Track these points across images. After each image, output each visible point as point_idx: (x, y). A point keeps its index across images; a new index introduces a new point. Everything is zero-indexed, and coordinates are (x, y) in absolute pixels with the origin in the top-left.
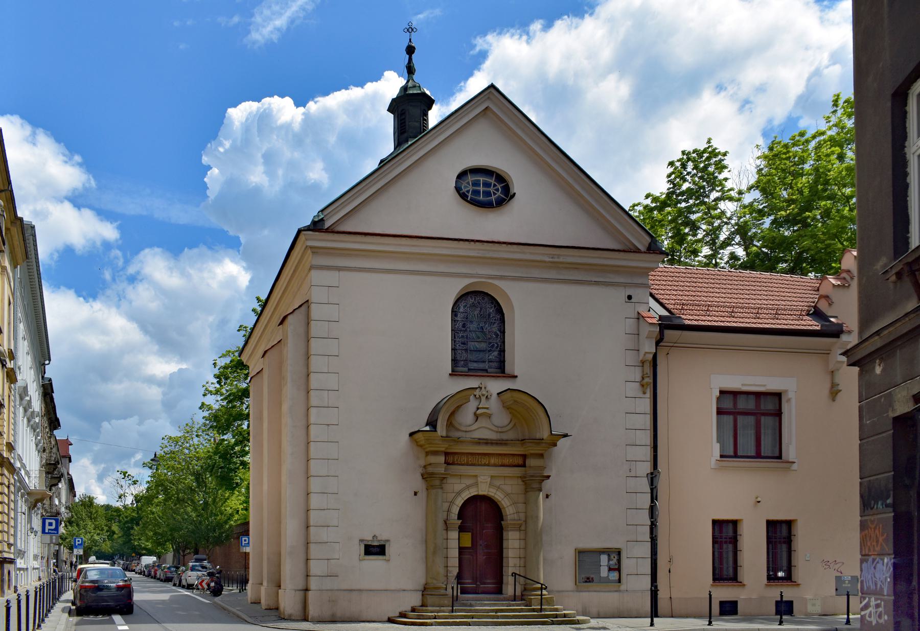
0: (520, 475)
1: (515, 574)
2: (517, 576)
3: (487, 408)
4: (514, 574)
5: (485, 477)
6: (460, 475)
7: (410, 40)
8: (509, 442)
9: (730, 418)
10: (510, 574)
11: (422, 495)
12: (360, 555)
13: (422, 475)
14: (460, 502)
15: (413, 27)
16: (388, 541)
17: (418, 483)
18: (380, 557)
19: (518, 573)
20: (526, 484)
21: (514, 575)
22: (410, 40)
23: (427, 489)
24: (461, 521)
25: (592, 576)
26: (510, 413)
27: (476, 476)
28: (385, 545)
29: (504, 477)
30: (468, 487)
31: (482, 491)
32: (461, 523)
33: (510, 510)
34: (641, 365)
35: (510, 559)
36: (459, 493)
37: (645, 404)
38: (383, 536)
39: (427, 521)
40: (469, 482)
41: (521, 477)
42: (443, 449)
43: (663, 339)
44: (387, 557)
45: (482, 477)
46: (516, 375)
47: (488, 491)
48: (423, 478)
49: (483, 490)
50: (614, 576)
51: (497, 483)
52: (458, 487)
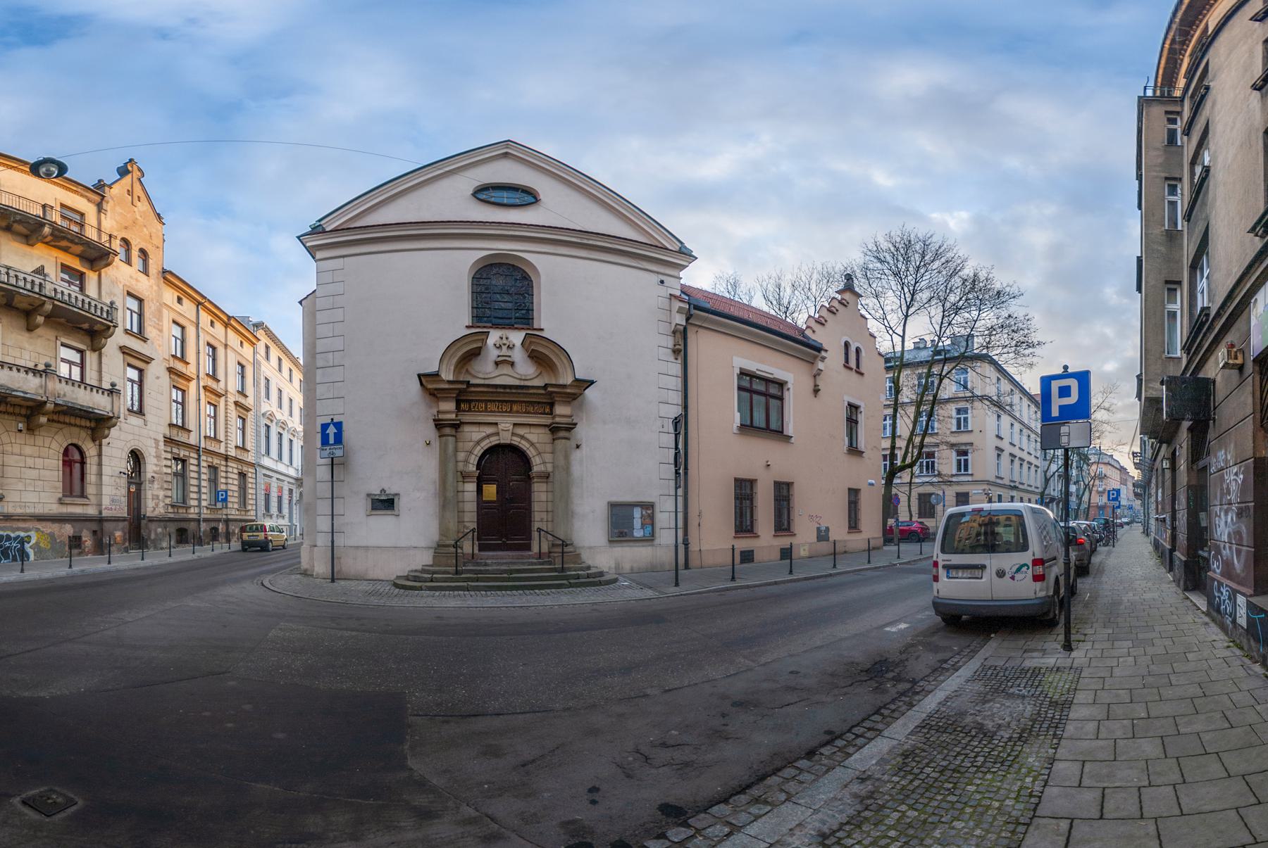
2: (542, 533)
3: (510, 356)
4: (539, 530)
5: (507, 425)
11: (436, 444)
14: (478, 451)
17: (430, 432)
18: (389, 512)
27: (496, 424)
36: (478, 443)
38: (392, 490)
40: (490, 430)
44: (396, 513)
45: (503, 425)
49: (506, 438)
51: (521, 431)
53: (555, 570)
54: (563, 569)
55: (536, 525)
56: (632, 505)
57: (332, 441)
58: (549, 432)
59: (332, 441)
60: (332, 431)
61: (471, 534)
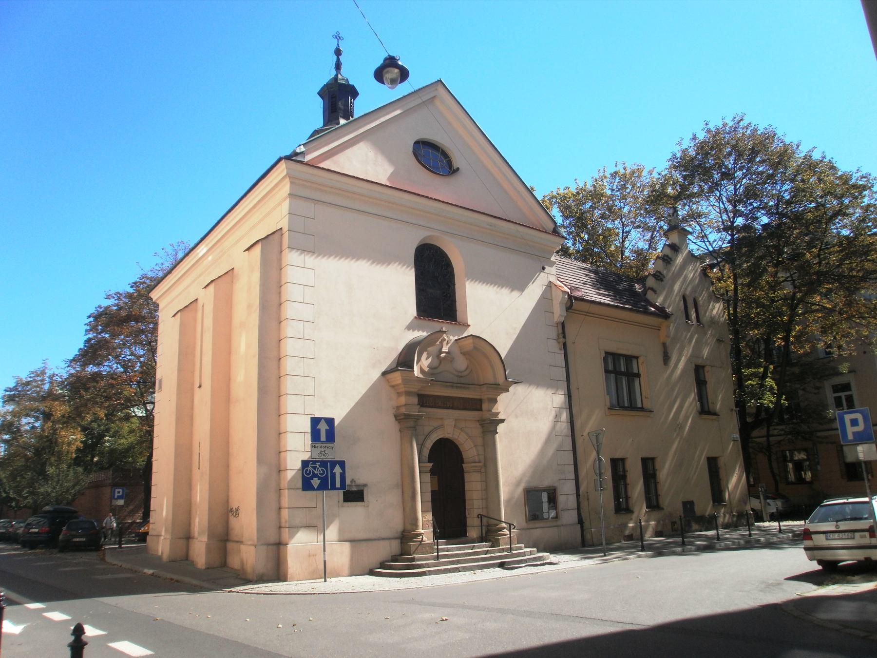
0: (478, 419)
1: (482, 516)
6: (429, 418)
7: (338, 44)
9: (613, 375)
10: (476, 515)
12: (339, 502)
13: (396, 416)
15: (340, 36)
16: (365, 485)
19: (485, 513)
20: (482, 427)
21: (480, 516)
22: (338, 44)
23: (400, 431)
24: (432, 464)
26: (467, 359)
27: (442, 419)
28: (363, 490)
30: (436, 429)
33: (469, 450)
35: (474, 501)
39: (402, 465)
41: (478, 421)
42: (416, 390)
43: (572, 307)
46: (469, 324)
47: (453, 434)
48: (396, 420)
50: (553, 514)
52: (427, 429)
53: (503, 550)
54: (511, 549)
56: (330, 490)
57: (323, 437)
58: (478, 426)
59: (323, 437)
60: (323, 427)
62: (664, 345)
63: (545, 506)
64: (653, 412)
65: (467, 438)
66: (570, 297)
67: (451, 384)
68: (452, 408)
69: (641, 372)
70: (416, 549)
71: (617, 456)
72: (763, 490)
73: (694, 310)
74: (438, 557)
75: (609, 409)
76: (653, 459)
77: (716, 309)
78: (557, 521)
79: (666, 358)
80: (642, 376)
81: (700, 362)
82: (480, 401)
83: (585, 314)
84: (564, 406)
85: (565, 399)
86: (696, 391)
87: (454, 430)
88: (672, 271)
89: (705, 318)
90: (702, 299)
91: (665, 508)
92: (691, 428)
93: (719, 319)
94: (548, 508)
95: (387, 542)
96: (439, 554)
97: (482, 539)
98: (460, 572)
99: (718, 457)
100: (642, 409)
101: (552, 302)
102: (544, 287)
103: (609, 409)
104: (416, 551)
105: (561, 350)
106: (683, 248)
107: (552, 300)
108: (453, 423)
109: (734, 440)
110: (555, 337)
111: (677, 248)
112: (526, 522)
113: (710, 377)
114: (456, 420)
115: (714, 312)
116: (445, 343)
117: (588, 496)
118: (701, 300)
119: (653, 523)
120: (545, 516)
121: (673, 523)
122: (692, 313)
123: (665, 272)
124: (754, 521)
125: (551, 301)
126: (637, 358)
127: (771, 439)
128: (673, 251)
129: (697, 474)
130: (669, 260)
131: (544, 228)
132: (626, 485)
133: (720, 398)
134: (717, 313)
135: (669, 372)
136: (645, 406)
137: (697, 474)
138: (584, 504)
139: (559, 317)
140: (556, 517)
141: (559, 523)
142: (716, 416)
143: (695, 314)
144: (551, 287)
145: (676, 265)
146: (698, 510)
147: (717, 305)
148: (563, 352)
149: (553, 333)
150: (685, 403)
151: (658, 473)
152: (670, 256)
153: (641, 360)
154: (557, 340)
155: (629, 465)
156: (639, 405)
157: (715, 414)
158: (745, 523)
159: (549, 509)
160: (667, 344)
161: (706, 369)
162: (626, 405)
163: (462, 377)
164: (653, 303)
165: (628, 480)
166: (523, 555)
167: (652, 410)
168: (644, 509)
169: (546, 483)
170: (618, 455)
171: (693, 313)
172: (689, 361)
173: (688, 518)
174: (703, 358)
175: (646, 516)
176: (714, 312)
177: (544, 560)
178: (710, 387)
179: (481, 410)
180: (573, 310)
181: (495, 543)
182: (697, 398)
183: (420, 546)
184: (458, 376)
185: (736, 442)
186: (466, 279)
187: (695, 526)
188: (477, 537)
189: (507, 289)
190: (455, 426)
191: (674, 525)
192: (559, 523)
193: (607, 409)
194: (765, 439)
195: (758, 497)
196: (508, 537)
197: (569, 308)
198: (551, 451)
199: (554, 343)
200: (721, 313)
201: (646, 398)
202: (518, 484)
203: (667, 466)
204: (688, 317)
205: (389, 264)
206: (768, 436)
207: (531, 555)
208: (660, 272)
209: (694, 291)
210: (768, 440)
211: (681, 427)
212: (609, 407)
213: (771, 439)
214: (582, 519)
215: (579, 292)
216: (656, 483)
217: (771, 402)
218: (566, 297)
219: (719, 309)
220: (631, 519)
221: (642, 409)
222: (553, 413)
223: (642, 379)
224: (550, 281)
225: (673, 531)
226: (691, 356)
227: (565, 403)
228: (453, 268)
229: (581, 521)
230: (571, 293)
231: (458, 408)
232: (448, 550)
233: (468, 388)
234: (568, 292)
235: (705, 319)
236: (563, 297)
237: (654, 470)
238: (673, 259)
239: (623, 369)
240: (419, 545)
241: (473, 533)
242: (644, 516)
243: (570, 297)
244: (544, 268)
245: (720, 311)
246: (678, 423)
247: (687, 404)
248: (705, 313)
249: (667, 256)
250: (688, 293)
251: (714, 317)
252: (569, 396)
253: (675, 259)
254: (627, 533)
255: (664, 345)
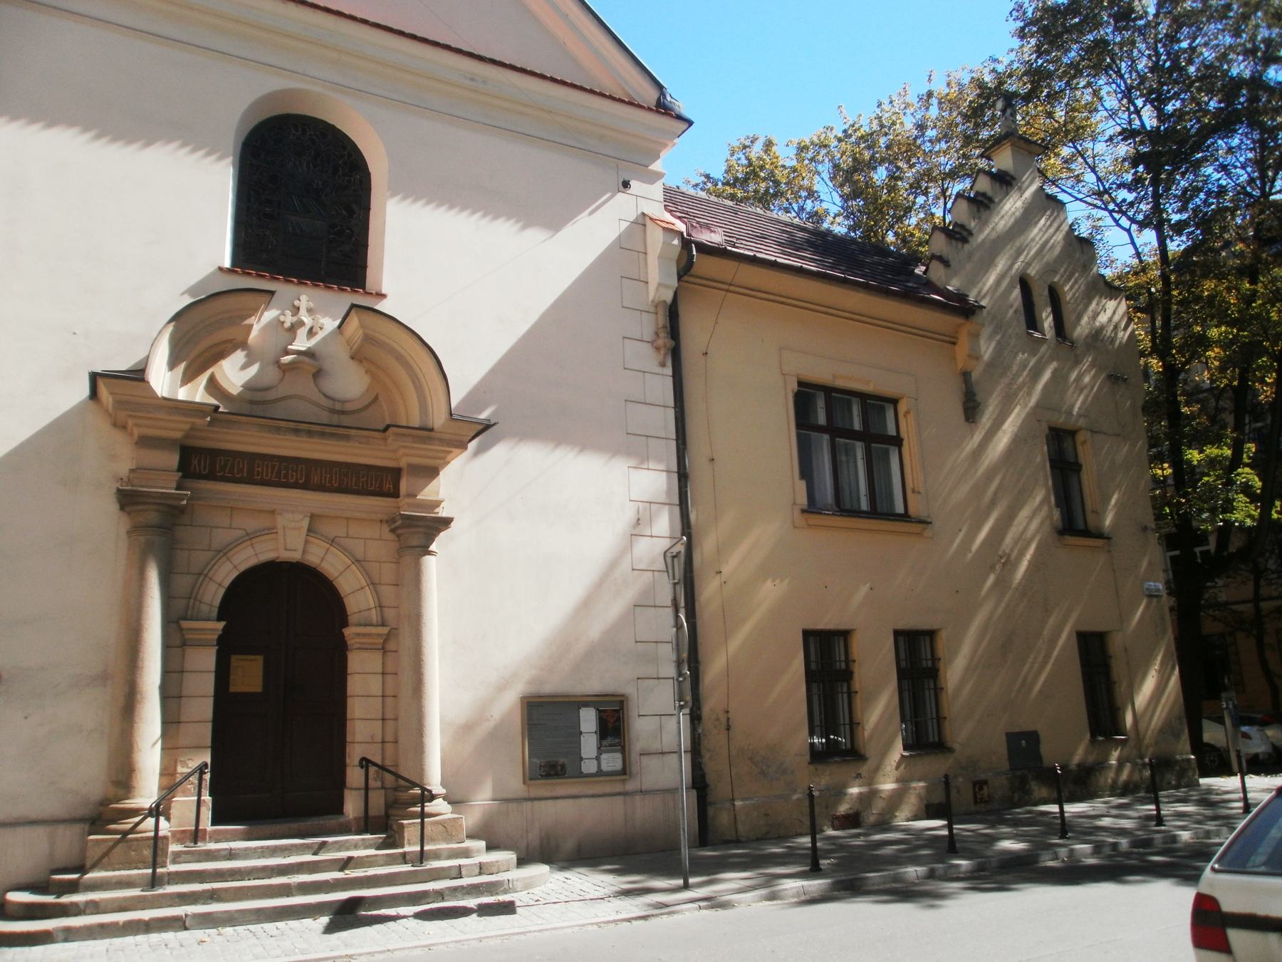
0: (381, 516)
2: (372, 770)
4: (365, 763)
8: (353, 432)
10: (356, 761)
19: (378, 760)
20: (398, 536)
21: (364, 762)
25: (561, 760)
26: (366, 372)
29: (348, 519)
31: (286, 549)
32: (223, 630)
34: (652, 310)
37: (663, 386)
46: (384, 292)
47: (304, 551)
50: (612, 761)
53: (404, 858)
54: (422, 856)
55: (354, 753)
58: (389, 535)
61: (194, 779)
62: (966, 375)
63: (589, 745)
64: (931, 523)
65: (349, 562)
66: (686, 243)
67: (292, 425)
68: (305, 486)
69: (903, 434)
70: (106, 854)
71: (821, 626)
72: (1231, 706)
73: (1049, 310)
74: (154, 881)
75: (803, 511)
76: (931, 634)
77: (1109, 313)
78: (624, 781)
79: (971, 409)
80: (905, 443)
81: (1060, 420)
82: (396, 473)
83: (732, 288)
84: (663, 498)
85: (669, 478)
86: (1050, 483)
87: (307, 542)
88: (994, 224)
89: (1079, 330)
90: (1072, 288)
91: (957, 747)
92: (1035, 566)
93: (1116, 334)
94: (599, 748)
95: (40, 833)
96: (159, 870)
97: (367, 824)
98: (186, 929)
99: (1110, 632)
100: (905, 517)
101: (646, 259)
102: (624, 225)
103: (803, 511)
104: (105, 860)
105: (663, 365)
106: (1024, 179)
107: (646, 253)
108: (305, 524)
109: (1150, 596)
110: (648, 333)
111: (1008, 178)
112: (524, 783)
113: (1095, 455)
114: (313, 516)
115: (1103, 318)
116: (302, 333)
117: (728, 719)
118: (1069, 291)
119: (922, 784)
120: (589, 767)
121: (979, 785)
122: (1044, 315)
123: (973, 225)
124: (1197, 777)
125: (642, 256)
126: (894, 402)
127: (1263, 605)
128: (998, 185)
129: (1049, 667)
130: (986, 201)
131: (629, 95)
132: (851, 694)
133: (1113, 501)
134: (1110, 320)
135: (978, 437)
136: (912, 511)
137: (1049, 667)
138: (715, 740)
139: (657, 289)
140: (624, 771)
141: (631, 786)
142: (1100, 540)
143: (1051, 318)
144: (645, 225)
145: (1003, 212)
146: (1050, 753)
147: (1111, 305)
148: (669, 371)
149: (647, 325)
150: (1021, 507)
151: (941, 665)
152: (990, 193)
153: (902, 407)
154: (652, 343)
155: (858, 646)
156: (900, 509)
157: (1099, 535)
158: (1173, 782)
159: (600, 750)
160: (975, 376)
161: (1080, 437)
162: (864, 505)
163: (343, 412)
164: (942, 287)
165: (856, 685)
166: (454, 873)
167: (929, 520)
168: (897, 751)
169: (594, 684)
170: (827, 622)
171: (1047, 317)
172: (1034, 415)
173: (1019, 773)
174: (1070, 413)
175: (903, 766)
176: (1103, 318)
177: (506, 892)
178: (1089, 478)
179: (396, 494)
180: (692, 276)
181: (393, 840)
182: (1053, 499)
183: (120, 846)
184: (332, 411)
185: (1155, 600)
186: (388, 194)
187: (1040, 791)
188: (355, 819)
189: (512, 221)
190: (309, 530)
191: (981, 789)
192: (631, 786)
193: (797, 512)
194: (1250, 605)
195: (1220, 720)
196: (148, 838)
197: (685, 270)
198: (613, 609)
199: (647, 349)
200: (1120, 321)
201: (913, 492)
202: (502, 687)
203: (965, 650)
204: (1032, 322)
205: (147, 145)
206: (1257, 599)
207: (480, 874)
208: (962, 226)
209: (1050, 269)
210: (1258, 609)
211: (1009, 564)
212: (805, 507)
213: (1263, 605)
214: (703, 776)
215: (713, 235)
216: (938, 691)
217: (1250, 516)
218: (676, 242)
219: (1114, 312)
220: (859, 776)
221: (905, 517)
222: (629, 514)
223: (905, 449)
224: (643, 214)
225: (976, 802)
226: (1037, 405)
227: (669, 492)
228: (370, 174)
229: (700, 783)
230: (689, 235)
231: (321, 488)
232: (231, 855)
233: (347, 438)
234: (682, 233)
235: (1081, 330)
236: (666, 244)
237: (935, 659)
238: (997, 200)
239: (857, 425)
240: (119, 841)
241: (352, 806)
242: (897, 768)
243: (686, 243)
244: (626, 185)
245: (1116, 318)
246: (1000, 553)
247: (1024, 513)
248: (1079, 317)
249: (984, 195)
250: (1032, 272)
251: (1102, 328)
252: (683, 476)
253: (1001, 201)
254: (843, 809)
255: (966, 375)
